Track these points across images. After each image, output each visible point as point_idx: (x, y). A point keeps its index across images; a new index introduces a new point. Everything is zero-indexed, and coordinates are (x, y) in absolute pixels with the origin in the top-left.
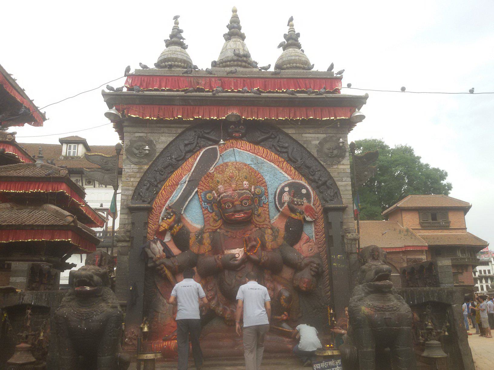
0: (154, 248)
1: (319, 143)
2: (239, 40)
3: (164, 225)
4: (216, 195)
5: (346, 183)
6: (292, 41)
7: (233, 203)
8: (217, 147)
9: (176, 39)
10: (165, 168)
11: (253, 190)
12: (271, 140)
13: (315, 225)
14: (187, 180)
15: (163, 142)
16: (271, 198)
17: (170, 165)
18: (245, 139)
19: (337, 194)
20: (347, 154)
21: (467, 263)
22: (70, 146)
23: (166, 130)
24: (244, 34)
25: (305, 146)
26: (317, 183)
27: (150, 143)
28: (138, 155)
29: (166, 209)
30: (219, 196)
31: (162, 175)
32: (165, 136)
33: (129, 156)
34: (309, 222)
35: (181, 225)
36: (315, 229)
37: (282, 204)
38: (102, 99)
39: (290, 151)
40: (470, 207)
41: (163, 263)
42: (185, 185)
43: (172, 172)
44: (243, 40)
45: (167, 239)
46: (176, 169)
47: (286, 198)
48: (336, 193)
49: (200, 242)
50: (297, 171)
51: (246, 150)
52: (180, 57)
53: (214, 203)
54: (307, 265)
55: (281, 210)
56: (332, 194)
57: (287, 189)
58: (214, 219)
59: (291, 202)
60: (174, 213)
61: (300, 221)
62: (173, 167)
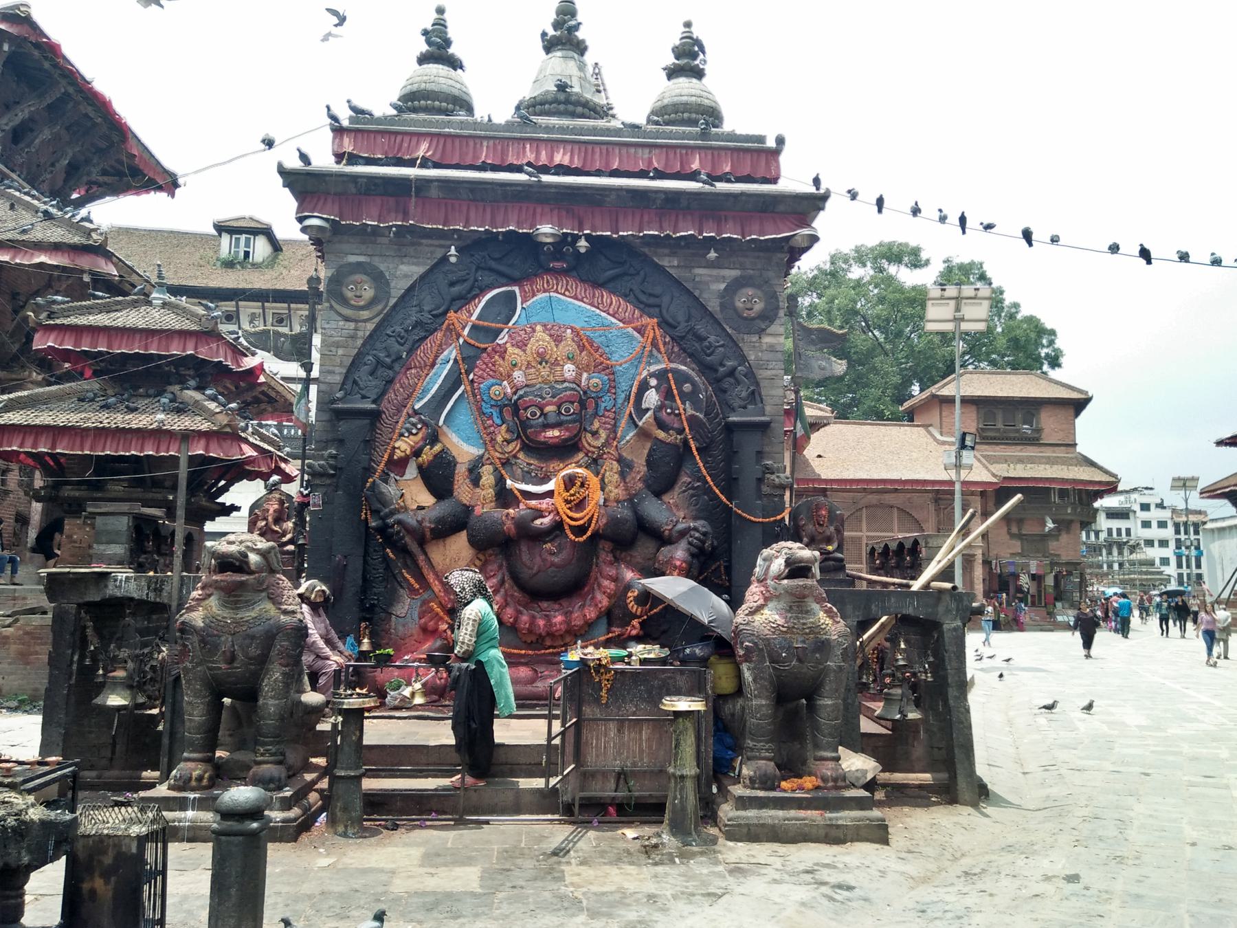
0: (382, 493)
2: (571, 53)
3: (403, 446)
4: (509, 390)
5: (774, 372)
6: (688, 59)
7: (542, 410)
8: (516, 289)
9: (438, 49)
12: (626, 278)
14: (453, 357)
15: (406, 276)
17: (418, 324)
18: (575, 274)
19: (755, 396)
20: (781, 313)
21: (1069, 517)
22: (238, 240)
24: (583, 41)
25: (697, 293)
26: (716, 371)
27: (379, 280)
28: (353, 302)
29: (409, 416)
30: (515, 393)
31: (402, 345)
33: (334, 304)
35: (437, 448)
37: (642, 412)
38: (280, 180)
39: (665, 300)
40: (1087, 401)
41: (399, 522)
42: (449, 366)
43: (426, 338)
44: (582, 54)
45: (411, 471)
46: (432, 332)
47: (652, 398)
48: (753, 393)
49: (476, 481)
50: (679, 345)
51: (576, 298)
52: (445, 88)
53: (506, 405)
54: (683, 533)
55: (640, 424)
56: (744, 394)
57: (653, 382)
58: (505, 440)
59: (660, 408)
60: (425, 424)
62: (426, 329)
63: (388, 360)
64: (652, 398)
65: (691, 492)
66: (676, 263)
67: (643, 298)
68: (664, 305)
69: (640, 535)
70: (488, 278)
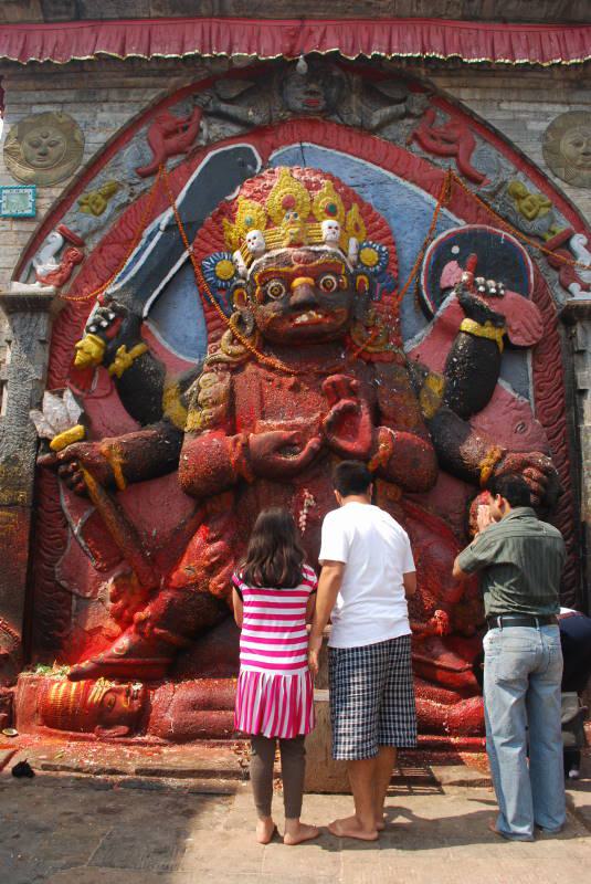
1: (549, 129)
4: (242, 264)
10: (109, 195)
11: (352, 250)
13: (536, 360)
15: (105, 125)
16: (407, 280)
18: (335, 118)
23: (114, 95)
26: (542, 239)
28: (34, 162)
30: (249, 267)
31: (95, 214)
32: (111, 110)
34: (522, 350)
35: (138, 349)
36: (535, 371)
51: (338, 149)
61: (495, 341)
63: (79, 235)
64: (454, 274)
65: (515, 413)
66: (478, 97)
67: (431, 143)
68: (461, 152)
69: (442, 477)
70: (211, 129)
